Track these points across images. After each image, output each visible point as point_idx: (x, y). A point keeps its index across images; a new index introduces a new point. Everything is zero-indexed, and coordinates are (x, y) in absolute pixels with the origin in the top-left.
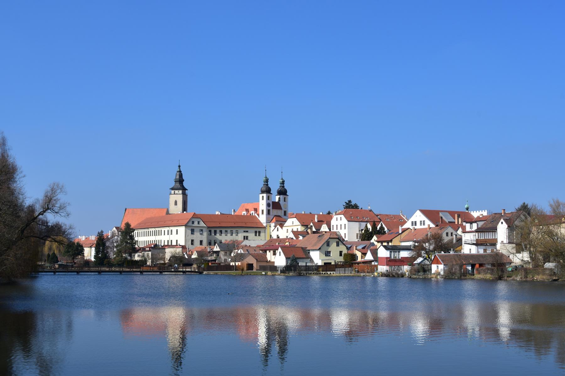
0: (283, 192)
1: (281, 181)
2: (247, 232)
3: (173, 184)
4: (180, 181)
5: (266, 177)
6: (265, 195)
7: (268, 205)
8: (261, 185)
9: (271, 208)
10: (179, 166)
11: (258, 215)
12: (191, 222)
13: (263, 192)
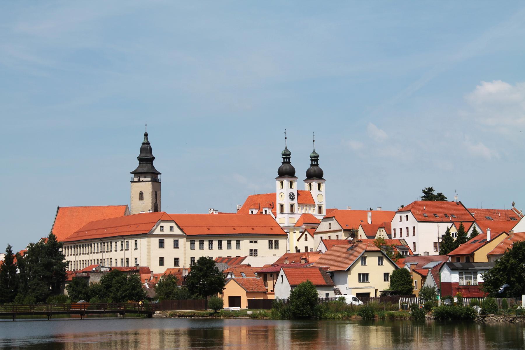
2: (256, 242)
3: (135, 165)
4: (146, 158)
5: (286, 149)
7: (292, 197)
8: (279, 162)
9: (295, 201)
10: (146, 135)
11: (275, 214)
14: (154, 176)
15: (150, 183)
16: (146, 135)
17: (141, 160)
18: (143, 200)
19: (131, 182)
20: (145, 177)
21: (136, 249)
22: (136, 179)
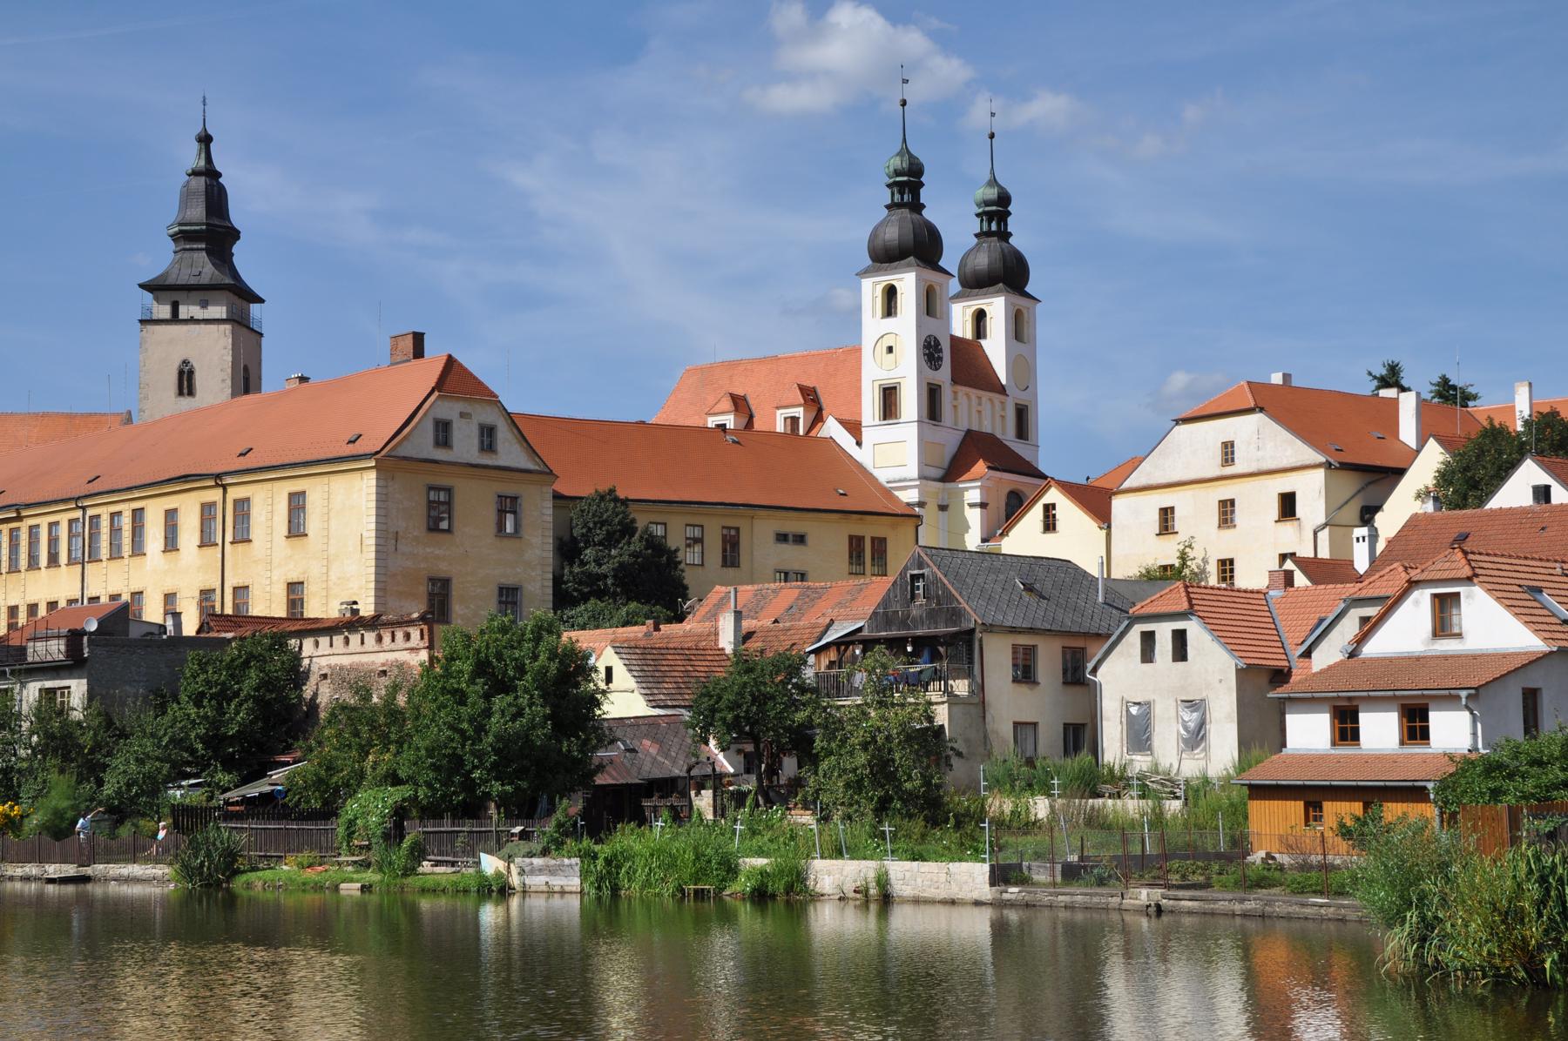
1: (992, 193)
2: (800, 539)
3: (160, 258)
5: (905, 151)
6: (907, 282)
9: (944, 375)
10: (205, 140)
11: (854, 428)
13: (885, 256)
14: (238, 301)
15: (228, 327)
16: (205, 140)
17: (184, 236)
18: (191, 393)
19: (142, 321)
20: (204, 304)
21: (296, 530)
22: (164, 311)
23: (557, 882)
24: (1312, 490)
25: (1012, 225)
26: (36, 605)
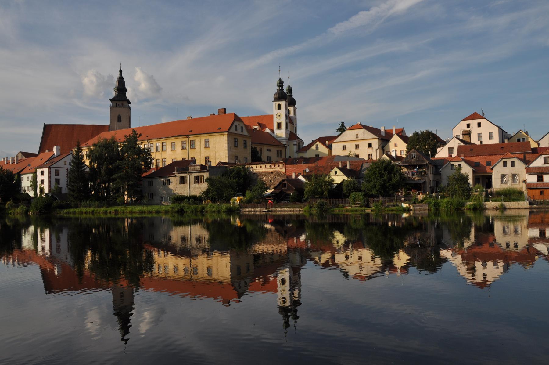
0: (292, 102)
2: (270, 150)
5: (280, 79)
6: (283, 103)
8: (275, 89)
9: (288, 121)
12: (234, 127)
23: (422, 208)
24: (375, 143)
25: (293, 94)
26: (453, 148)
